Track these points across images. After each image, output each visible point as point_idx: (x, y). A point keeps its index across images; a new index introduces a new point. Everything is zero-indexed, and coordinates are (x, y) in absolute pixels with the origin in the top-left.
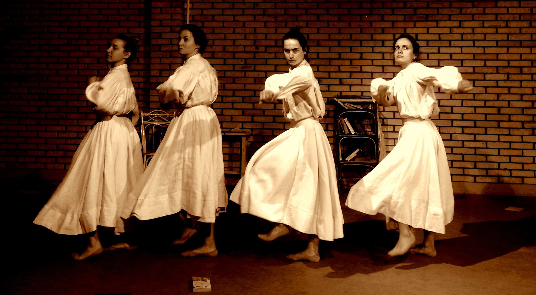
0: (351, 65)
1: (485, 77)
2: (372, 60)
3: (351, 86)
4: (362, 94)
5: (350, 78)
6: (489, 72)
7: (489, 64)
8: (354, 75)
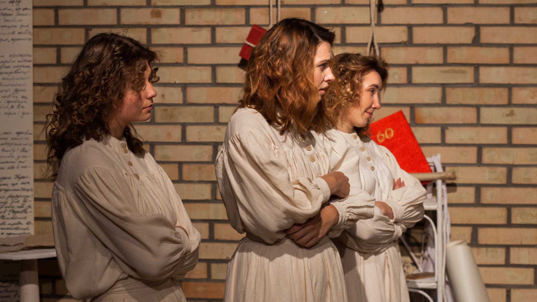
0: (445, 64)
3: (444, 128)
5: (444, 103)
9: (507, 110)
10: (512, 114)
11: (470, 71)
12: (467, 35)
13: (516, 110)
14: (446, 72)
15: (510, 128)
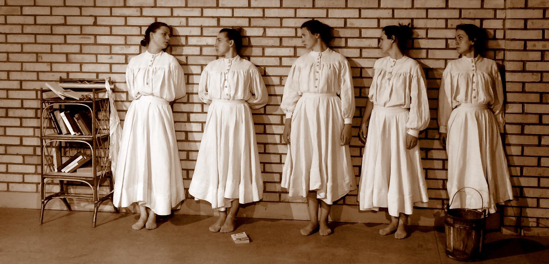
1: (263, 53)
2: (111, 27)
3: (81, 64)
4: (97, 77)
5: (81, 53)
6: (270, 45)
7: (269, 32)
8: (86, 49)
9: (109, 56)
10: (111, 58)
11: (93, 37)
12: (91, 21)
13: (113, 56)
14: (82, 38)
15: (111, 64)
